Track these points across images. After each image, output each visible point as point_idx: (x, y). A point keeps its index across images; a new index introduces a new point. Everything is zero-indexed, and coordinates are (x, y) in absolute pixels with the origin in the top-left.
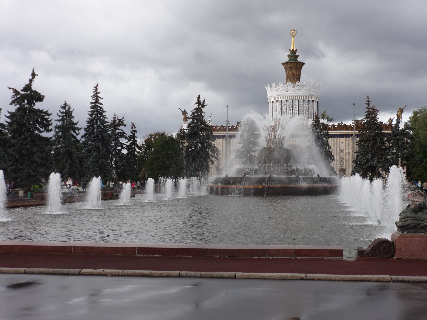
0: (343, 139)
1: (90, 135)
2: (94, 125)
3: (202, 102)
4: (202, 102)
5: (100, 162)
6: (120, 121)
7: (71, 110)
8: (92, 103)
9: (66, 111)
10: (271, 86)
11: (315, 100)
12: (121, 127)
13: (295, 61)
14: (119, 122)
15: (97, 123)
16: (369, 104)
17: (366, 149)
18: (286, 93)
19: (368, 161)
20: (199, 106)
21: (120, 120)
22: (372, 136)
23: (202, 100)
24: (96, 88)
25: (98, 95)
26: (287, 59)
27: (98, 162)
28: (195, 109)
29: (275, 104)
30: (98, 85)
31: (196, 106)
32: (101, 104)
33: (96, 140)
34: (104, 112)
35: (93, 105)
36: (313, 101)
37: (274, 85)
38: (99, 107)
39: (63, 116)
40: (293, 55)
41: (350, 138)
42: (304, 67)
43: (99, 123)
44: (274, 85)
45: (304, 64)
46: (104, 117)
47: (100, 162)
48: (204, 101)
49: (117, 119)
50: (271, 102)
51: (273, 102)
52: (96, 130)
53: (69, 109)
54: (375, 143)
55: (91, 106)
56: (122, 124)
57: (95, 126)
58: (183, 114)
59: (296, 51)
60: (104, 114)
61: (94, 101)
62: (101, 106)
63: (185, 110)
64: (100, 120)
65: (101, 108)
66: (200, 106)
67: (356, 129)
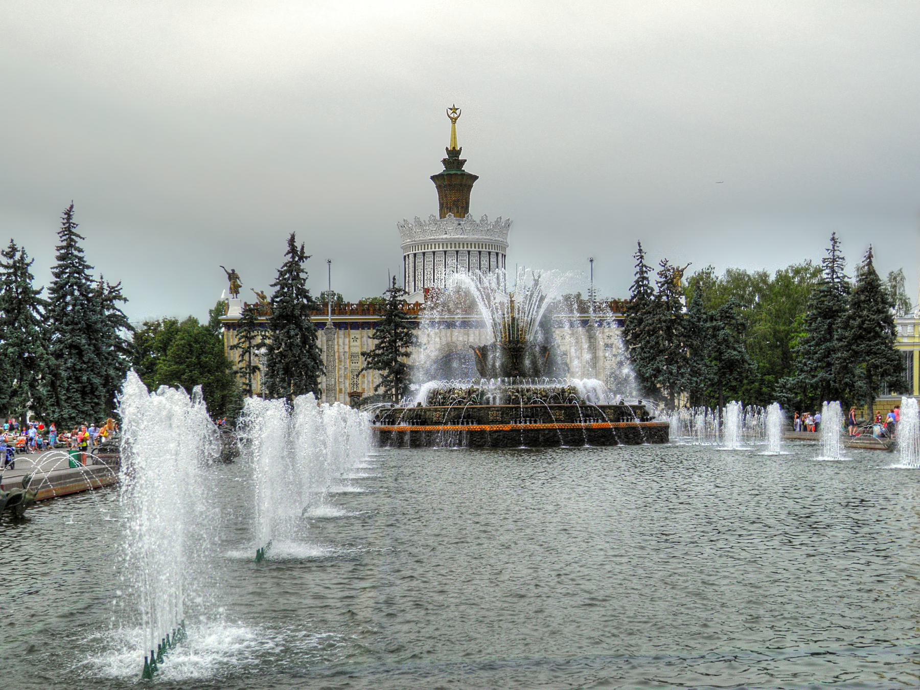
1: (56, 320)
2: (64, 296)
3: (299, 249)
4: (299, 249)
5: (85, 378)
6: (112, 289)
7: (27, 261)
8: (59, 248)
9: (15, 262)
11: (501, 252)
12: (117, 304)
13: (459, 173)
14: (110, 292)
15: (72, 294)
16: (642, 257)
17: (651, 347)
18: (445, 236)
20: (293, 257)
21: (113, 288)
22: (665, 322)
23: (298, 245)
24: (69, 214)
25: (73, 230)
26: (440, 169)
27: (78, 380)
28: (285, 265)
29: (420, 260)
30: (72, 207)
31: (289, 258)
32: (80, 251)
33: (73, 330)
34: (88, 267)
35: (63, 251)
36: (497, 254)
38: (76, 256)
39: (9, 275)
40: (454, 159)
43: (76, 293)
45: (476, 178)
46: (87, 279)
47: (85, 378)
48: (303, 247)
49: (105, 286)
50: (411, 257)
51: (415, 255)
52: (70, 308)
53: (22, 258)
55: (58, 254)
56: (118, 297)
57: (68, 298)
58: (230, 278)
59: (459, 152)
60: (87, 272)
61: (64, 244)
62: (80, 255)
63: (233, 271)
64: (80, 286)
65: (80, 259)
66: (297, 259)
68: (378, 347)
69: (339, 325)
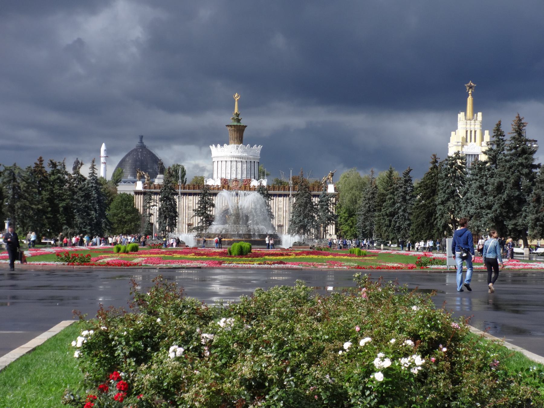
0: (281, 199)
10: (216, 146)
13: (238, 124)
19: (300, 221)
29: (220, 163)
37: (219, 145)
41: (287, 198)
42: (246, 129)
44: (219, 145)
50: (216, 162)
54: (305, 207)
61: (91, 172)
65: (96, 177)
67: (294, 189)
68: (199, 207)
69: (184, 194)
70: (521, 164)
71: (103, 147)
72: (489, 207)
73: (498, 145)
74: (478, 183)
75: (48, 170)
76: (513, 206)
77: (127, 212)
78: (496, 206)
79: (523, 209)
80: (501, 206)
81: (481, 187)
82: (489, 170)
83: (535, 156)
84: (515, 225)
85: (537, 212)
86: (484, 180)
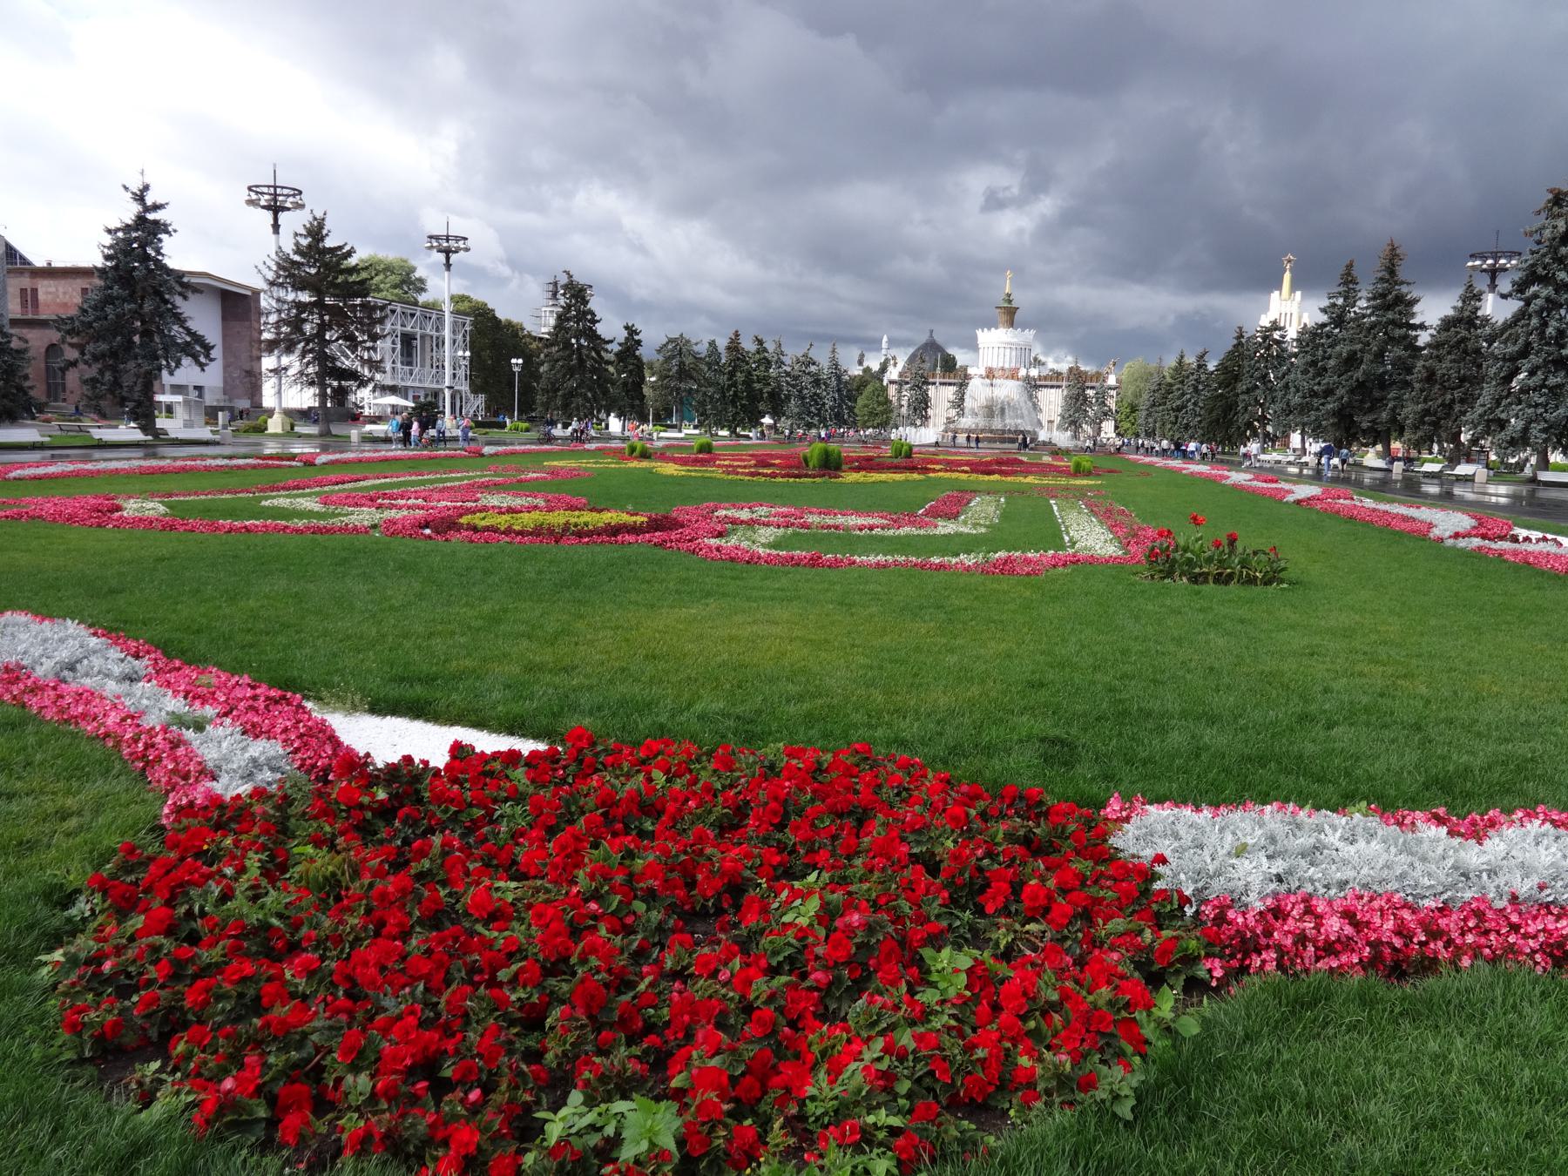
70: (1393, 322)
71: (885, 339)
72: (1329, 392)
73: (1346, 299)
74: (1309, 358)
75: (748, 345)
76: (1370, 392)
77: (879, 403)
78: (1340, 392)
79: (1391, 395)
80: (1352, 391)
81: (1314, 363)
82: (1328, 337)
83: (1416, 309)
84: (1373, 421)
85: (1425, 401)
86: (1320, 352)
